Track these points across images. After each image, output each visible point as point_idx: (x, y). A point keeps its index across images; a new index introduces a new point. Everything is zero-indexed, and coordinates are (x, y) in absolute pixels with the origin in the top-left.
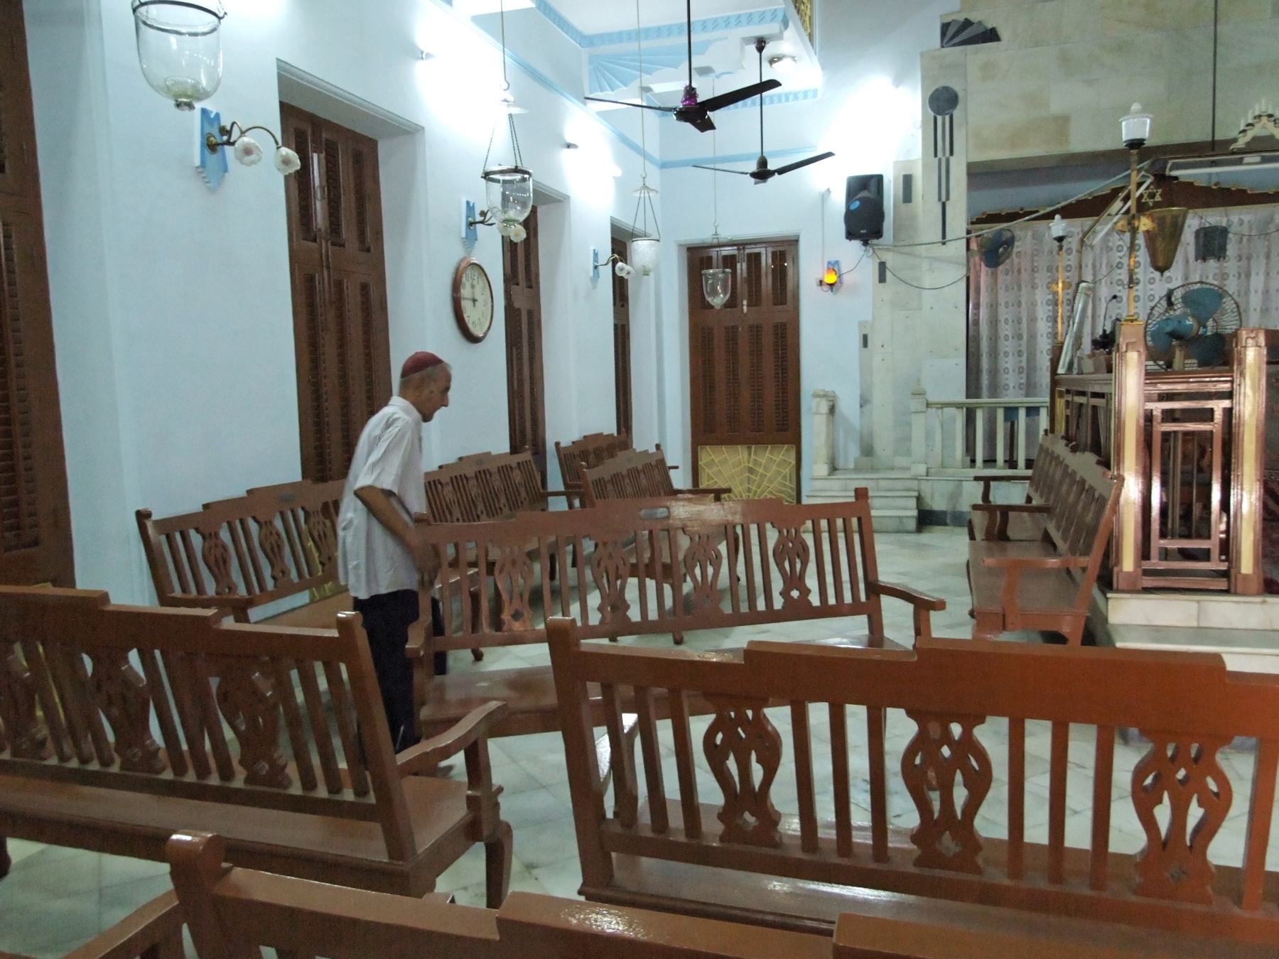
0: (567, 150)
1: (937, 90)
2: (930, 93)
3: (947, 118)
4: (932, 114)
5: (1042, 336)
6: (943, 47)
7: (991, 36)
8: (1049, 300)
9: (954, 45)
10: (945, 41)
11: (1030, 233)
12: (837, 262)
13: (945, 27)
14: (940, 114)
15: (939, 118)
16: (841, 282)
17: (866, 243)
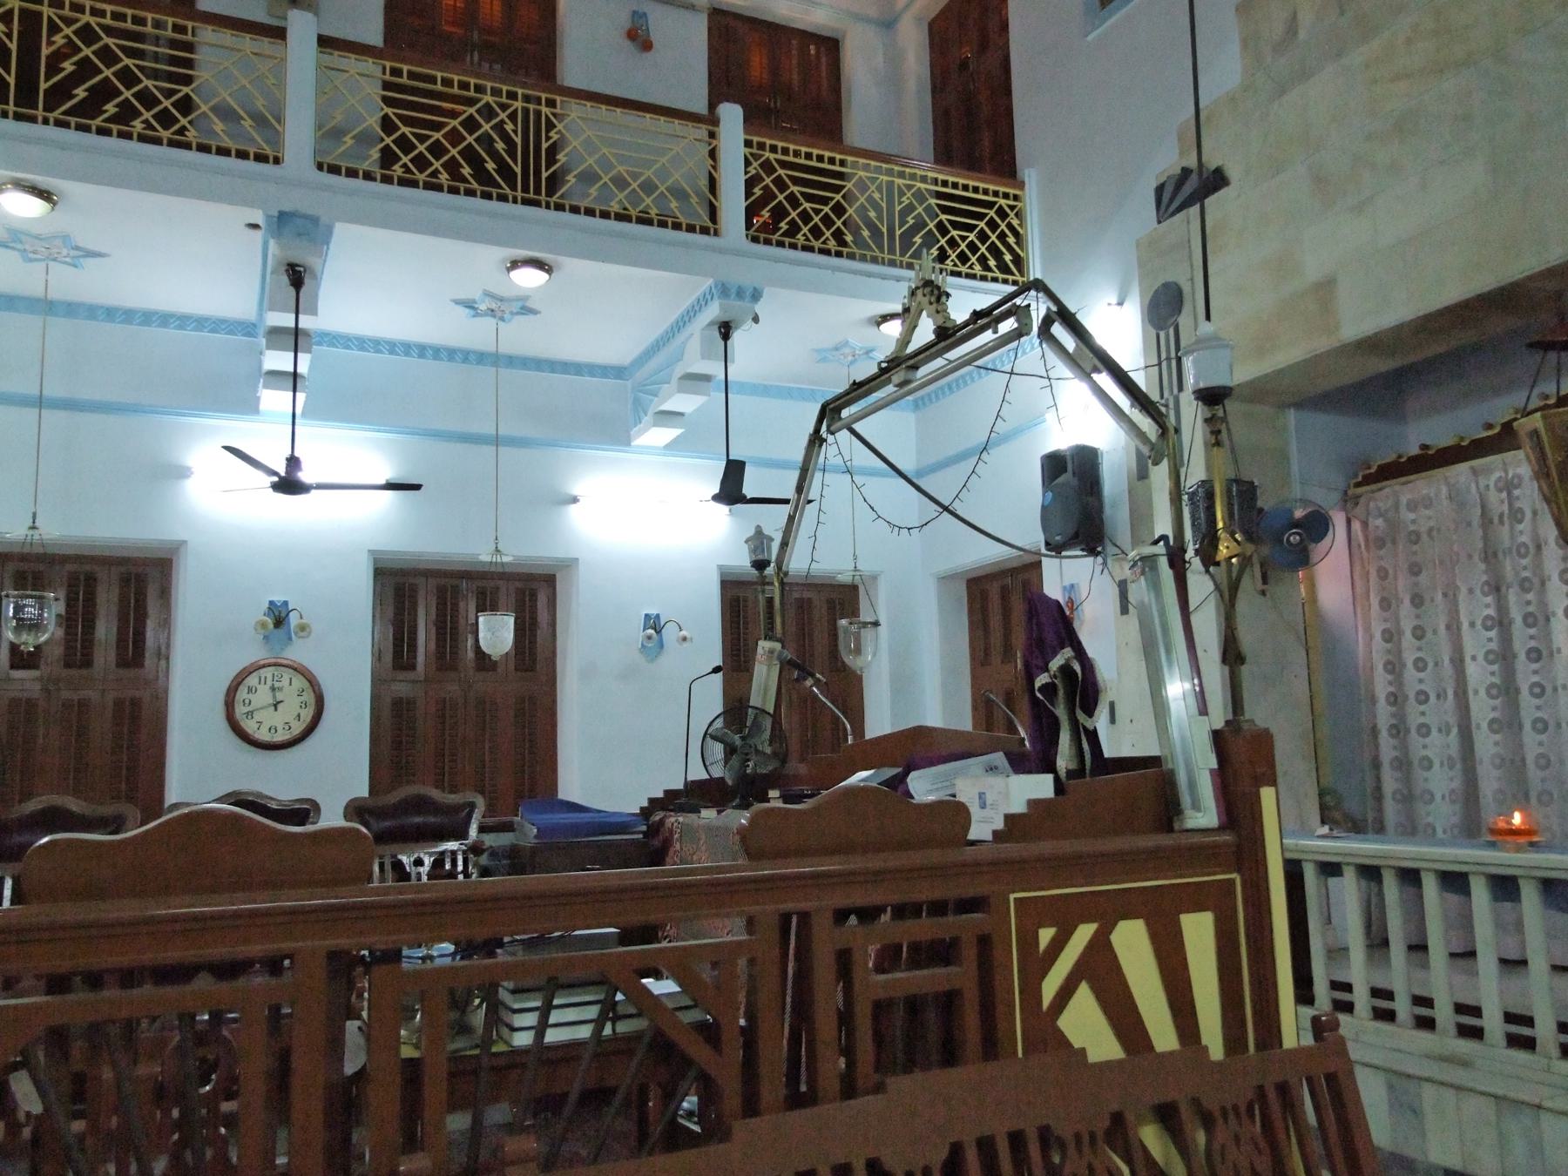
0: (573, 506)
1: (1156, 292)
2: (1147, 302)
3: (1171, 331)
4: (1153, 332)
5: (1476, 692)
6: (1159, 222)
7: (1216, 180)
8: (1487, 617)
9: (1173, 214)
10: (1161, 212)
11: (1444, 490)
12: (1072, 586)
13: (1160, 190)
14: (1162, 330)
15: (1162, 334)
16: (1079, 618)
17: (1092, 552)
